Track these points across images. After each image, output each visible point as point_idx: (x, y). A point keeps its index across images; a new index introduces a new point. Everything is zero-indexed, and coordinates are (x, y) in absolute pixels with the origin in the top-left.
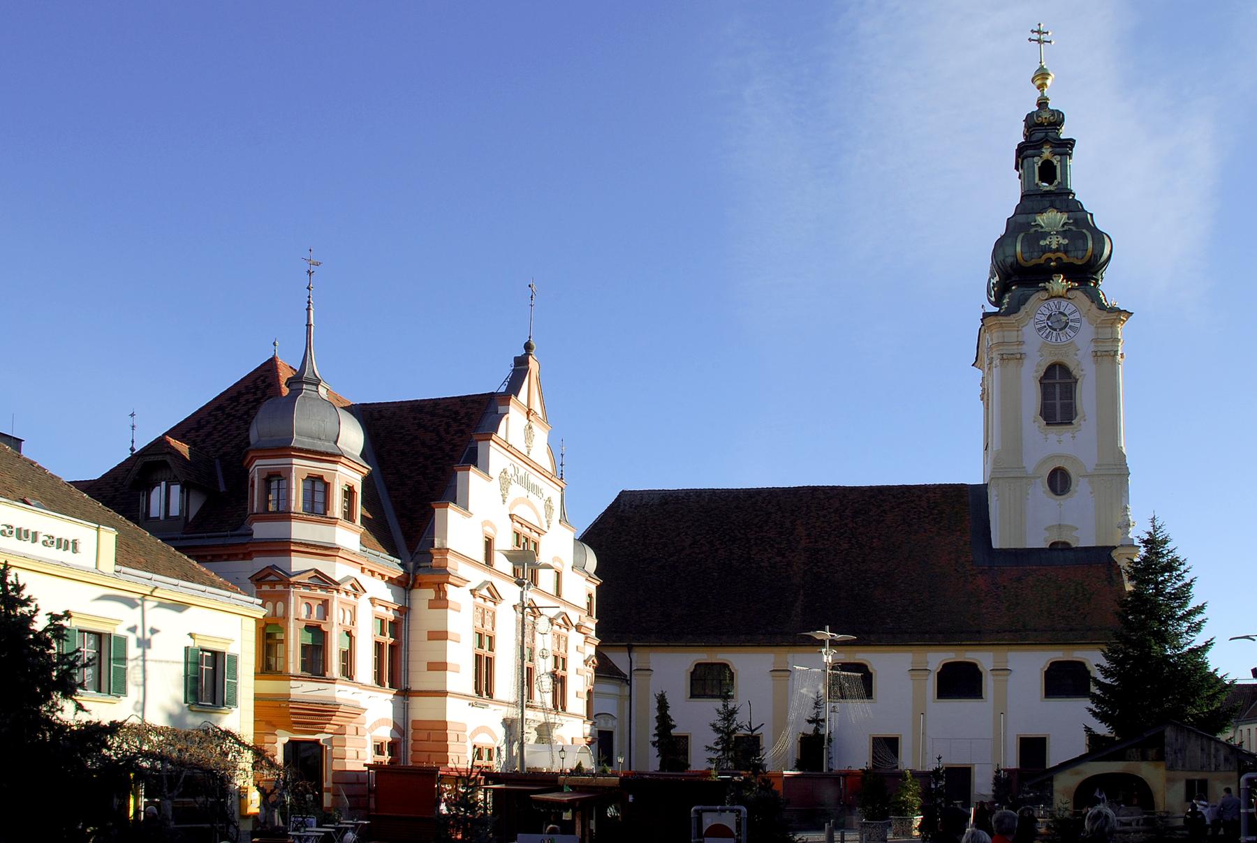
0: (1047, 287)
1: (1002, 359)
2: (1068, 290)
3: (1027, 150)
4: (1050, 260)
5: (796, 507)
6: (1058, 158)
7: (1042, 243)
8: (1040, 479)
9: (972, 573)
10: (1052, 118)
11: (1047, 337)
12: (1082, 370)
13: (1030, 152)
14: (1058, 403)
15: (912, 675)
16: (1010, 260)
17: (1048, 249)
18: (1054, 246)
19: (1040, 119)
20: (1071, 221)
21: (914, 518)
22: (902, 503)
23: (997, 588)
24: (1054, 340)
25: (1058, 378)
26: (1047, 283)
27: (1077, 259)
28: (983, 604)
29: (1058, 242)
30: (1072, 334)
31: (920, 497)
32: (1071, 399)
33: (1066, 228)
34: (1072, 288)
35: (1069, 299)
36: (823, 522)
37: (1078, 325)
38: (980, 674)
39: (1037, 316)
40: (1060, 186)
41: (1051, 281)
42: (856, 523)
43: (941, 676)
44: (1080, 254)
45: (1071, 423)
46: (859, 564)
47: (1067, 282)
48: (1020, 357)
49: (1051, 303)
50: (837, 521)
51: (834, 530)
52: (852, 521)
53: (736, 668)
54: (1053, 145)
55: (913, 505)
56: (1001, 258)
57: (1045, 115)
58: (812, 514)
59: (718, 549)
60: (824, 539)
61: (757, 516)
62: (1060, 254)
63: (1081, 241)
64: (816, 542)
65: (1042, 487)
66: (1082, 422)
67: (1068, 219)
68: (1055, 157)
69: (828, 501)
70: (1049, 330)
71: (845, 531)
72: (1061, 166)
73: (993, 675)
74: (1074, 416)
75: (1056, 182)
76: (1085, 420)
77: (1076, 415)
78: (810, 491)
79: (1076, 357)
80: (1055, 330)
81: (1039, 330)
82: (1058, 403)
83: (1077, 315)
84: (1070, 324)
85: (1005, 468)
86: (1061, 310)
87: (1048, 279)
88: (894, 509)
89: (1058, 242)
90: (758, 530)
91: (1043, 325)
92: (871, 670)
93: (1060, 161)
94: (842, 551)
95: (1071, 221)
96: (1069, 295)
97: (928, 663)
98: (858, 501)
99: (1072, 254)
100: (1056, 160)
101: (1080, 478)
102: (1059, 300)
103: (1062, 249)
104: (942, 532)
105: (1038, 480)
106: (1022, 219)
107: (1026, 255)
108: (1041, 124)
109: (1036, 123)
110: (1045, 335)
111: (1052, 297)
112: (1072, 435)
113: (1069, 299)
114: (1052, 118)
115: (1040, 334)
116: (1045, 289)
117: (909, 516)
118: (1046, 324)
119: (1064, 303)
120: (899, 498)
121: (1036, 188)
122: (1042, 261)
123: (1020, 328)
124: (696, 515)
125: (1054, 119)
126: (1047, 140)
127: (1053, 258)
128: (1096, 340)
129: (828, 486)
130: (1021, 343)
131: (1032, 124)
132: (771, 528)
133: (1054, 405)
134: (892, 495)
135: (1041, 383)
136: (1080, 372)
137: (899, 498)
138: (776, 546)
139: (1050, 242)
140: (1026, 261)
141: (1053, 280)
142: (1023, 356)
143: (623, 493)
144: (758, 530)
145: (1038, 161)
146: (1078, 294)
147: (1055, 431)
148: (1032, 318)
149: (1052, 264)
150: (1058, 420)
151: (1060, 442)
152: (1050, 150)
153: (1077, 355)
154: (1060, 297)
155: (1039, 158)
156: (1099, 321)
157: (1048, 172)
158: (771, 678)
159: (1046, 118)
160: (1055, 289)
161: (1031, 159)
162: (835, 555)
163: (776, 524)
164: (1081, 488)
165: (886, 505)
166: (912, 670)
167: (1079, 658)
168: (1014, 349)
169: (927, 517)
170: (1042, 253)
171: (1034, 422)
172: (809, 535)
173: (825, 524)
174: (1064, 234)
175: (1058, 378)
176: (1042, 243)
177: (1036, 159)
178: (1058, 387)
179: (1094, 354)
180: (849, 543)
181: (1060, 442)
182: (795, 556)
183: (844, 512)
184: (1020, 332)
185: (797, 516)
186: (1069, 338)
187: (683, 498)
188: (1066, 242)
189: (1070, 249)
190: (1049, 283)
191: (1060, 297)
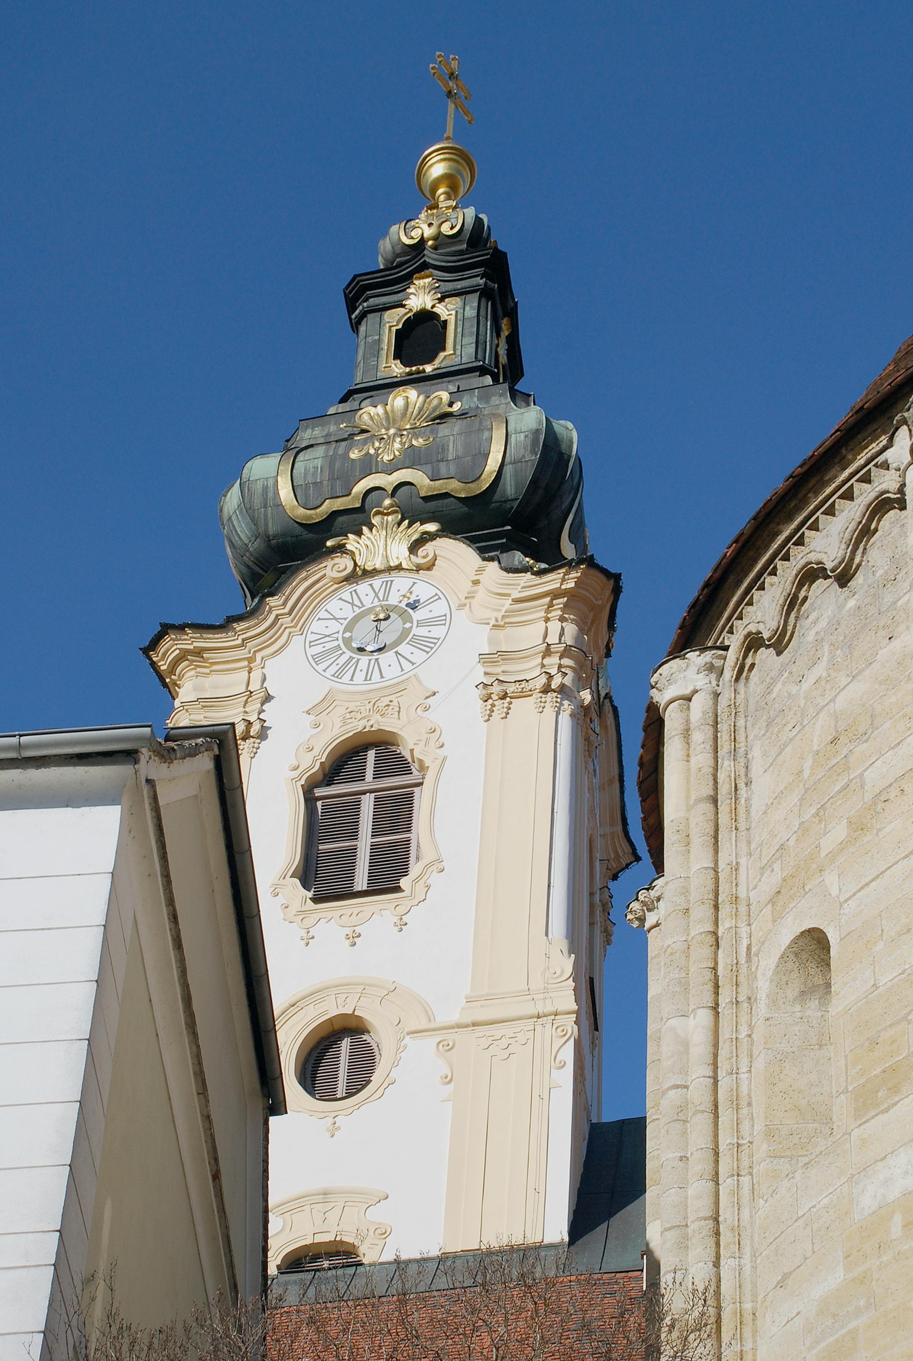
11: (338, 675)
24: (360, 677)
30: (418, 656)
37: (438, 631)
39: (317, 626)
83: (440, 608)
84: (415, 631)
91: (335, 643)
102: (385, 577)
115: (320, 668)
118: (340, 642)
141: (371, 527)
186: (407, 666)
190: (359, 533)
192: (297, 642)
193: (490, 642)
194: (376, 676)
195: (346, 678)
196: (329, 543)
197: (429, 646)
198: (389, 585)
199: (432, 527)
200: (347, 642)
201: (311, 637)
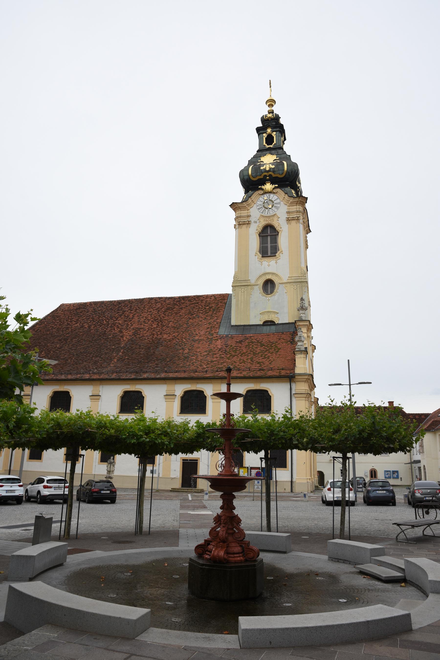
0: (263, 188)
1: (239, 225)
2: (274, 189)
3: (260, 131)
4: (265, 176)
5: (139, 307)
6: (275, 133)
7: (262, 168)
8: (258, 286)
9: (216, 338)
10: (273, 116)
11: (262, 212)
12: (281, 228)
13: (261, 132)
14: (269, 245)
15: (166, 399)
16: (246, 178)
17: (265, 171)
18: (268, 169)
19: (267, 117)
20: (278, 158)
21: (195, 311)
22: (193, 304)
23: (227, 347)
24: (266, 213)
25: (269, 233)
26: (263, 186)
27: (280, 174)
28: (216, 356)
29: (270, 167)
30: (276, 210)
31: (202, 300)
32: (276, 243)
33: (275, 161)
34: (275, 188)
35: (274, 193)
36: (149, 314)
37: (279, 205)
38: (206, 397)
39: (258, 203)
40: (276, 145)
41: (265, 185)
42: (165, 315)
43: (183, 398)
44: (281, 172)
45: (275, 256)
46: (157, 336)
47: (272, 185)
48: (249, 223)
49: (265, 196)
50: (156, 314)
51: (152, 318)
52: (163, 314)
53: (73, 394)
54: (272, 128)
55: (197, 305)
56: (242, 177)
57: (270, 115)
58: (144, 311)
59: (92, 330)
60: (145, 323)
61: (118, 313)
62: (270, 173)
63: (281, 166)
64: (141, 324)
65: (258, 291)
66: (281, 255)
67: (277, 158)
68: (273, 133)
69: (155, 304)
70: (264, 208)
71: (157, 319)
72: (276, 136)
73: (212, 399)
74: (277, 251)
75: (273, 144)
76: (282, 254)
77: (279, 250)
78: (149, 300)
79: (277, 221)
80: (267, 208)
81: (259, 209)
82: (269, 245)
83: (278, 201)
84: (275, 205)
85: (239, 281)
86: (271, 199)
87: (264, 184)
88: (187, 307)
89: (270, 167)
90: (115, 319)
91: (261, 206)
92: (143, 395)
93: (276, 134)
94: (152, 329)
95: (278, 158)
96: (274, 191)
97: (175, 391)
98: (170, 304)
99: (277, 173)
100: (274, 134)
101: (280, 285)
102: (269, 194)
103: (272, 170)
104: (207, 318)
105: (257, 287)
106: (254, 160)
107: (253, 175)
108: (268, 120)
109: (265, 120)
110: (261, 212)
111: (266, 193)
112: (275, 262)
113: (274, 193)
114: (273, 116)
115: (259, 211)
116: (262, 189)
117: (193, 310)
119: (272, 195)
120: (192, 301)
121: (264, 147)
122: (262, 177)
123: (249, 209)
124: (90, 313)
125: (273, 117)
126: (269, 125)
127: (268, 175)
128: (288, 213)
129: (158, 297)
130: (249, 216)
131: (264, 120)
132: (122, 318)
133: (267, 247)
134: (189, 300)
135: (260, 236)
136: (280, 229)
137: (192, 301)
138: (120, 327)
139: (265, 167)
140: (254, 177)
141: (266, 185)
142: (250, 222)
143: (62, 305)
144: (115, 319)
145: (265, 135)
146: (278, 190)
147: (266, 260)
148: (255, 204)
149: (267, 178)
150: (269, 254)
151: (269, 265)
152: (271, 130)
153: (278, 221)
154: (270, 192)
155: (266, 134)
156: (290, 202)
157: (270, 140)
158: (90, 400)
159: (270, 117)
160: (267, 189)
161: (262, 134)
162: (147, 331)
163: (125, 316)
164: (279, 290)
165: (184, 305)
166: (167, 395)
167: (264, 387)
168: (246, 220)
169: (202, 310)
170: (261, 173)
171: (256, 256)
172: (139, 321)
173: (149, 316)
174: (272, 164)
175: (269, 233)
176: (262, 168)
177: (264, 135)
178: (269, 238)
179: (287, 219)
180: (157, 325)
181: (269, 265)
182: (127, 332)
183: (161, 309)
184: (249, 211)
185: (137, 312)
186: (274, 212)
187: (88, 306)
188: (273, 167)
189: (275, 170)
190: (264, 186)
191: (270, 192)
192: (255, 205)
193: (288, 209)
194: (269, 214)
195: (264, 213)
196: (259, 187)
197: (277, 208)
198: (270, 196)
199: (277, 185)
200: (264, 206)
201: (257, 205)
